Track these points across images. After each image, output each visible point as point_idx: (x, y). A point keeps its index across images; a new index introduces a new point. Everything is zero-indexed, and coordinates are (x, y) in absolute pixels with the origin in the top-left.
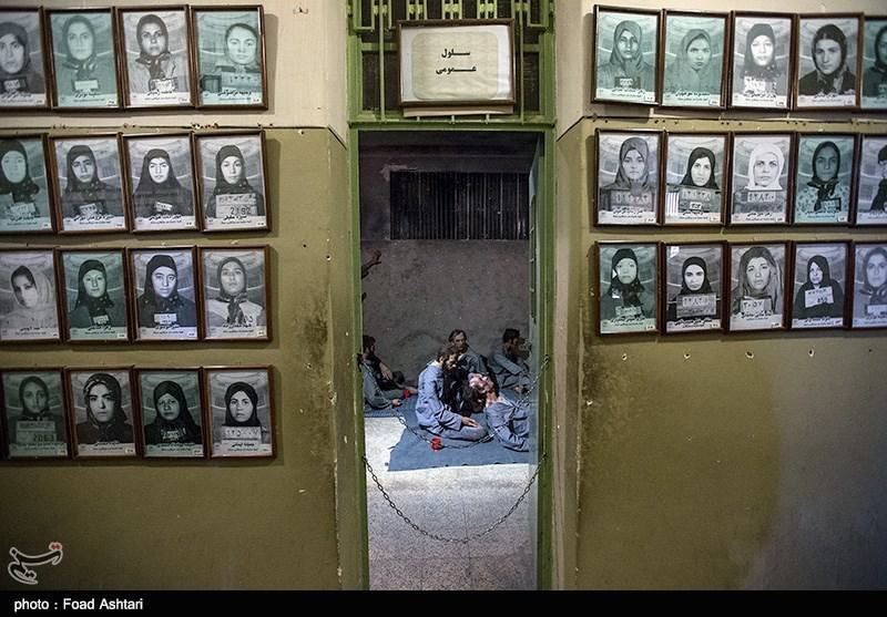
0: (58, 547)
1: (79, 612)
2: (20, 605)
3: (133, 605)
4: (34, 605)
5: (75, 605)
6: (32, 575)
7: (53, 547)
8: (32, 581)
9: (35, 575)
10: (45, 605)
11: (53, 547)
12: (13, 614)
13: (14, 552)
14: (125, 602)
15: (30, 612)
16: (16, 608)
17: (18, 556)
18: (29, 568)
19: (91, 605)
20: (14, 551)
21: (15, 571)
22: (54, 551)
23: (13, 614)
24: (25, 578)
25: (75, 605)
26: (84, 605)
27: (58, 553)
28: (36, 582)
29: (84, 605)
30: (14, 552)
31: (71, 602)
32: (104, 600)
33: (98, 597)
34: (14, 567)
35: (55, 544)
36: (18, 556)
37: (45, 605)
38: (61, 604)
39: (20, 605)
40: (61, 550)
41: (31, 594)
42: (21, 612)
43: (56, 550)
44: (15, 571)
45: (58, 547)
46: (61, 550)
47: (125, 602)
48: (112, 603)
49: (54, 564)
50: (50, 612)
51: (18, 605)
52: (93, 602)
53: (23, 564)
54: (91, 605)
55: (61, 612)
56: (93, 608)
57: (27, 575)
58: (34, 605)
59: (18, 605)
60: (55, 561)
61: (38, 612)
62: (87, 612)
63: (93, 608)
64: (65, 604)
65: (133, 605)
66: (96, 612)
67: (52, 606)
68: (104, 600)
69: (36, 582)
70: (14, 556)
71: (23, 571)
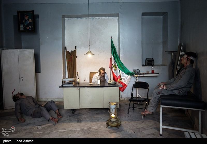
0: (14, 128)
1: (19, 143)
2: (5, 141)
3: (31, 141)
4: (8, 141)
5: (18, 141)
6: (7, 134)
7: (12, 128)
8: (8, 136)
9: (8, 134)
10: (11, 141)
11: (12, 128)
12: (3, 143)
13: (3, 129)
14: (29, 140)
15: (7, 143)
16: (4, 142)
17: (4, 130)
18: (6, 132)
19: (21, 141)
20: (3, 129)
21: (4, 133)
22: (12, 129)
23: (3, 143)
24: (5, 134)
25: (18, 141)
26: (20, 141)
27: (13, 129)
28: (8, 136)
29: (20, 141)
30: (3, 129)
31: (17, 140)
32: (24, 140)
33: (23, 139)
34: (3, 132)
35: (13, 127)
36: (4, 130)
37: (11, 141)
38: (14, 141)
39: (5, 141)
40: (14, 128)
41: (7, 139)
42: (5, 143)
43: (13, 128)
44: (4, 133)
45: (14, 128)
46: (14, 128)
47: (29, 140)
48: (26, 141)
49: (13, 132)
50: (12, 143)
51: (4, 141)
52: (22, 140)
53: (6, 132)
54: (21, 141)
55: (14, 143)
56: (22, 142)
57: (6, 134)
58: (8, 141)
59: (4, 141)
60: (13, 131)
61: (9, 143)
62: (20, 143)
63: (22, 142)
64: (15, 141)
65: (31, 141)
66: (22, 143)
67: (12, 141)
68: (24, 140)
69: (8, 136)
70: (3, 130)
71: (5, 133)
